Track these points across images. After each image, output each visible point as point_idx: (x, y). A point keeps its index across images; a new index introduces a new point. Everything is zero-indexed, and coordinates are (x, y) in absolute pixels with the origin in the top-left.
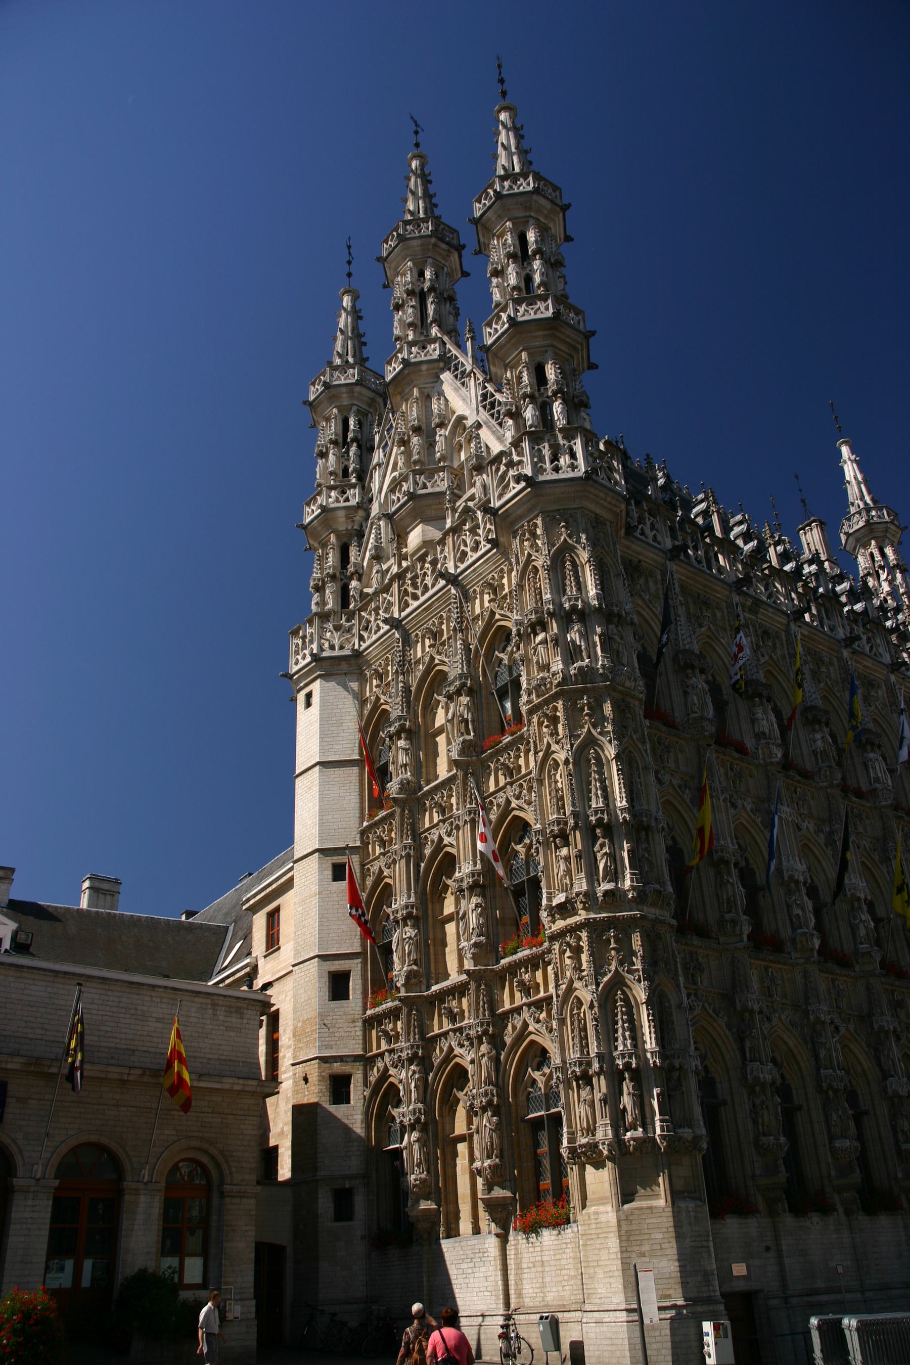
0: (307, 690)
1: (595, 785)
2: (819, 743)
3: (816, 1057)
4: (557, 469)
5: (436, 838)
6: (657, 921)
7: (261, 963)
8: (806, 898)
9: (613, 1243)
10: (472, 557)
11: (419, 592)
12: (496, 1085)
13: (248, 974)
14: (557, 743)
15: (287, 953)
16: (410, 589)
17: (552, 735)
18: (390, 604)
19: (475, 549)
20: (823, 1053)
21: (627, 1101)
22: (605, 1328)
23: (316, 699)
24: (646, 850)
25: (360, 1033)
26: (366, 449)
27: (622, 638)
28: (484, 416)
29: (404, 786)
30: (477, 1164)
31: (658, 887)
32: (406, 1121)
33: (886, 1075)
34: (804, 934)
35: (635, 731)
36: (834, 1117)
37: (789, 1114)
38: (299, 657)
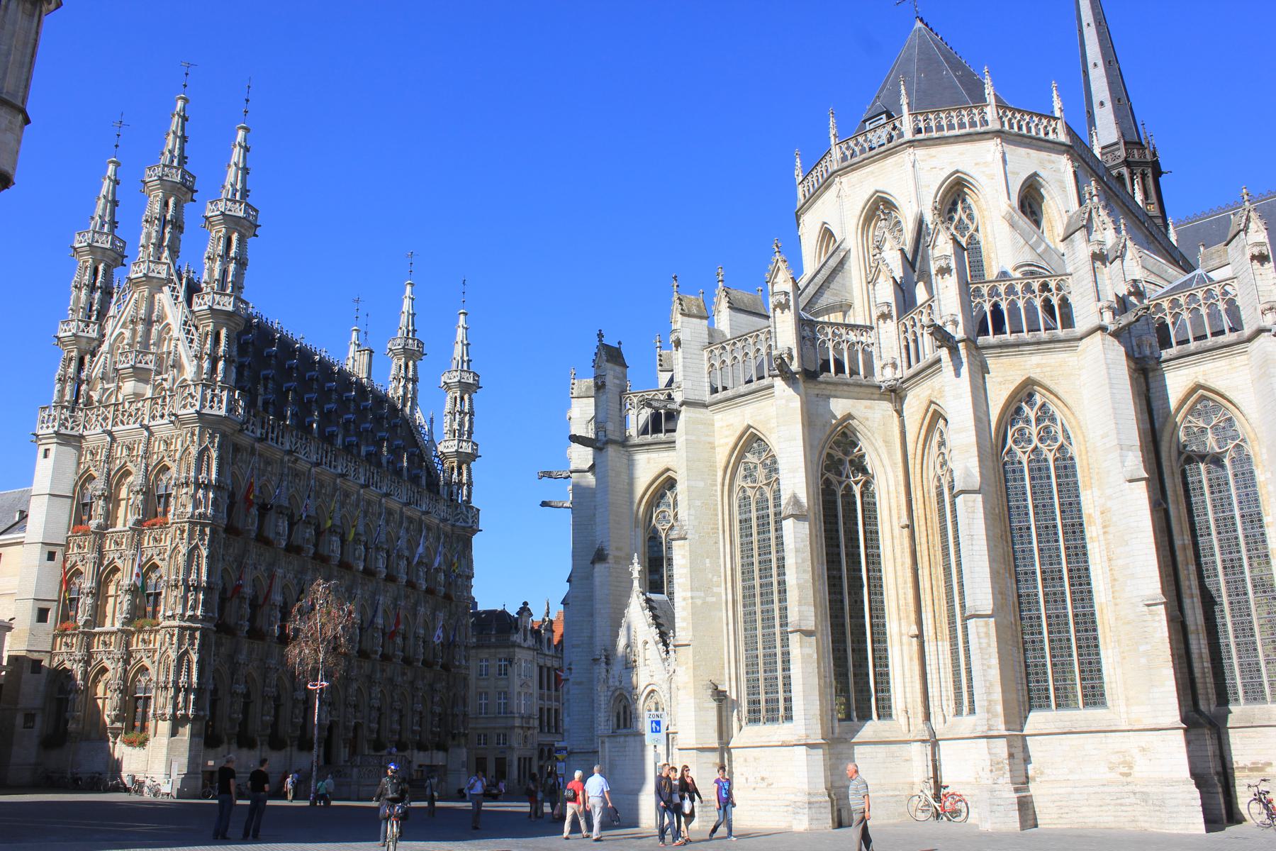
1: (194, 567)
4: (211, 407)
9: (165, 751)
18: (105, 419)
19: (162, 416)
21: (180, 699)
23: (52, 454)
26: (107, 293)
28: (183, 335)
29: (99, 526)
37: (246, 705)
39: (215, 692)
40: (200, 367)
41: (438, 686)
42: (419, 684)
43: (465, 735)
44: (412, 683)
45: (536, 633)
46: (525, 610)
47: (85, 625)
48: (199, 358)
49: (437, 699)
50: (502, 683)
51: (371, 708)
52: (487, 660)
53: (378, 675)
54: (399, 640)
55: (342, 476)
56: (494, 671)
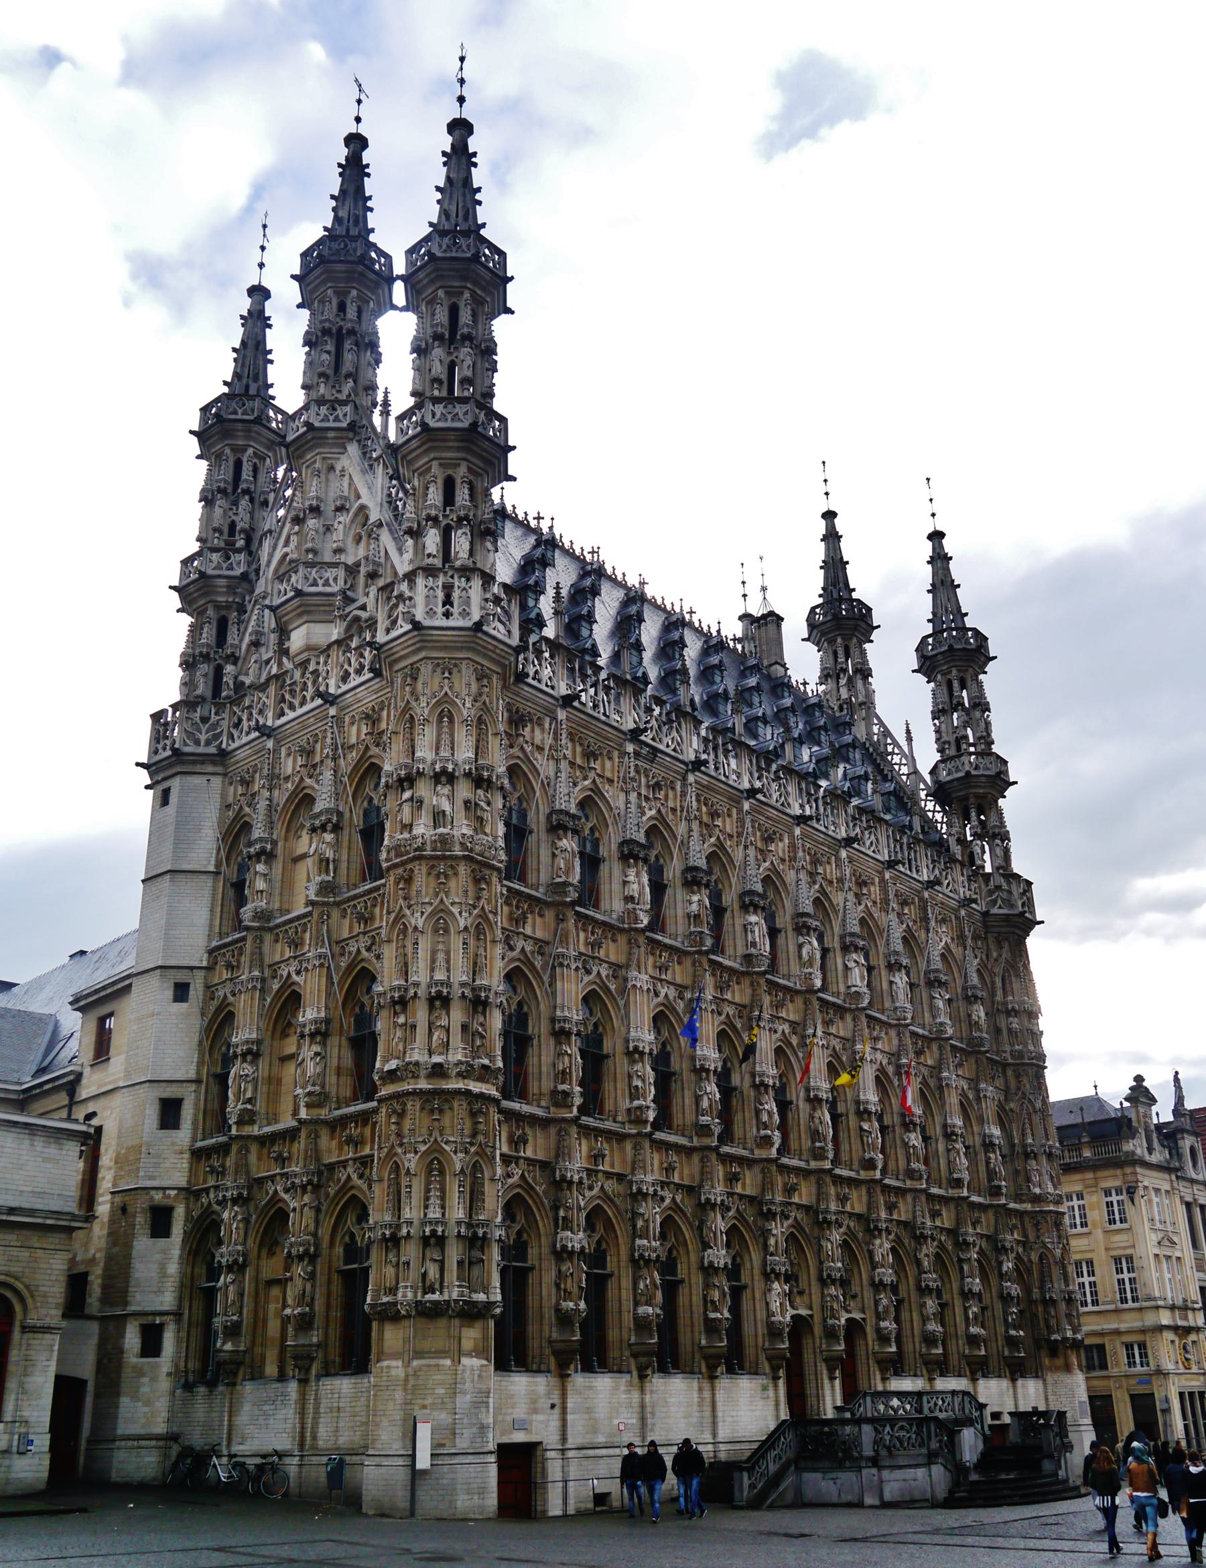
0: (165, 785)
1: (441, 956)
2: (694, 907)
3: (634, 1226)
5: (285, 974)
6: (482, 1096)
7: (87, 1071)
8: (648, 1068)
9: (399, 1395)
10: (355, 680)
11: (296, 703)
12: (315, 1235)
13: (70, 1082)
14: (409, 907)
15: (117, 1069)
16: (287, 696)
17: (405, 899)
19: (359, 672)
20: (640, 1223)
22: (382, 1470)
23: (173, 798)
24: (482, 1025)
25: (186, 1165)
27: (489, 804)
30: (288, 1311)
31: (486, 1062)
32: (224, 1261)
33: (706, 1246)
34: (640, 1108)
35: (489, 901)
36: (642, 1286)
38: (160, 747)
39: (515, 1250)
40: (419, 549)
41: (1010, 1238)
42: (970, 1233)
43: (1076, 1345)
44: (953, 1233)
45: (1168, 1135)
46: (1140, 1093)
47: (239, 1123)
48: (416, 534)
49: (1008, 1266)
50: (1120, 1240)
51: (878, 1286)
52: (1080, 1196)
53: (883, 1215)
54: (915, 1139)
55: (752, 793)
56: (1097, 1215)
